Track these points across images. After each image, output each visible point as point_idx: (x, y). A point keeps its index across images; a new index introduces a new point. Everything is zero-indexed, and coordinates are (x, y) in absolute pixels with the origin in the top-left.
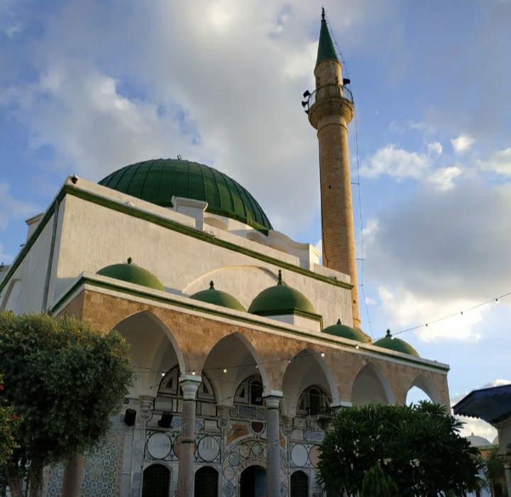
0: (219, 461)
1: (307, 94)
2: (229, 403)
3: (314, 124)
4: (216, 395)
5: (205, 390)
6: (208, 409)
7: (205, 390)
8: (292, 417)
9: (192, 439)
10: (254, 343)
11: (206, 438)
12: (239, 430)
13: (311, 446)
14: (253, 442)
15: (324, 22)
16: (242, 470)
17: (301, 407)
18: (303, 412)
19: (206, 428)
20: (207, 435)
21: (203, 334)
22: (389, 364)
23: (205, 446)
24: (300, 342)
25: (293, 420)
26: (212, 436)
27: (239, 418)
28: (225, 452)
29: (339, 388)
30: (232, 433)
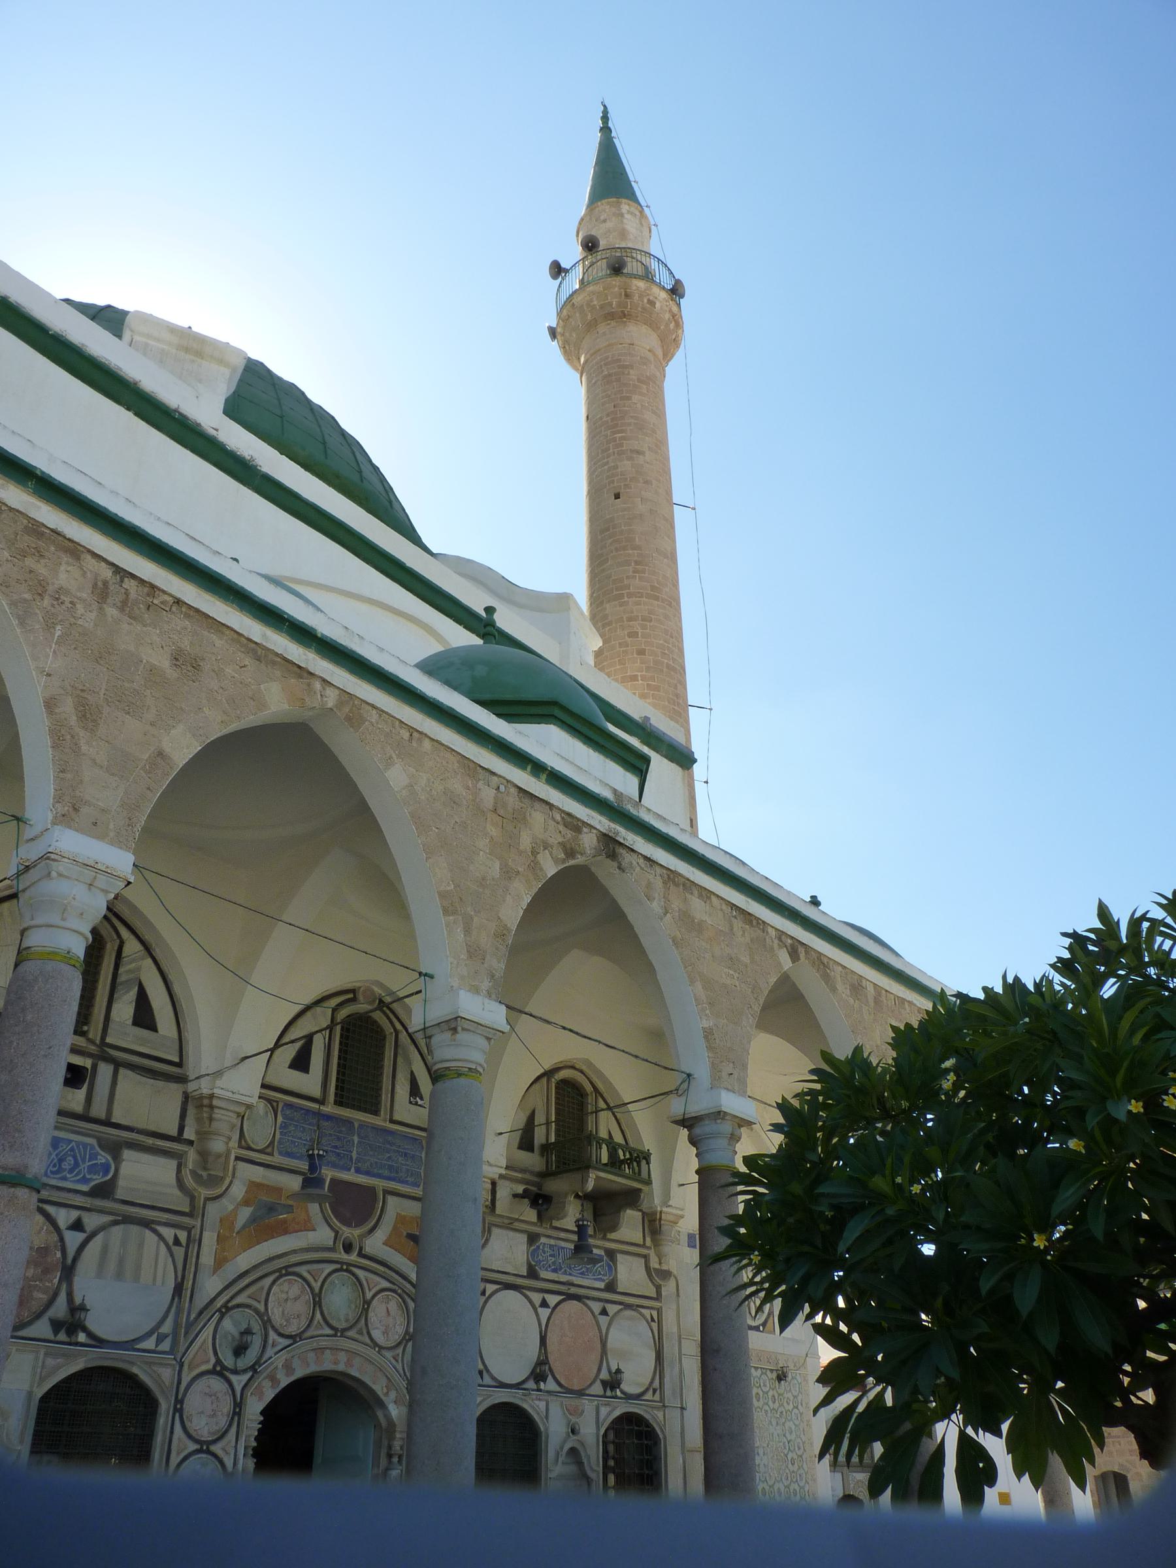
0: (166, 1346)
1: (557, 270)
2: (242, 1085)
3: (570, 352)
4: (190, 1050)
5: (144, 1017)
6: (142, 1103)
7: (144, 1017)
8: (493, 1172)
9: (36, 1166)
10: (397, 776)
11: (117, 1231)
12: (271, 1209)
13: (552, 1300)
14: (330, 1268)
15: (606, 129)
16: (270, 1394)
17: (526, 1144)
18: (533, 1161)
19: (121, 1183)
20: (127, 1220)
21: (171, 673)
22: (857, 986)
23: (112, 1266)
24: (574, 825)
25: (494, 1184)
26: (146, 1224)
27: (277, 1159)
28: (200, 1302)
29: (708, 1034)
30: (246, 1213)
